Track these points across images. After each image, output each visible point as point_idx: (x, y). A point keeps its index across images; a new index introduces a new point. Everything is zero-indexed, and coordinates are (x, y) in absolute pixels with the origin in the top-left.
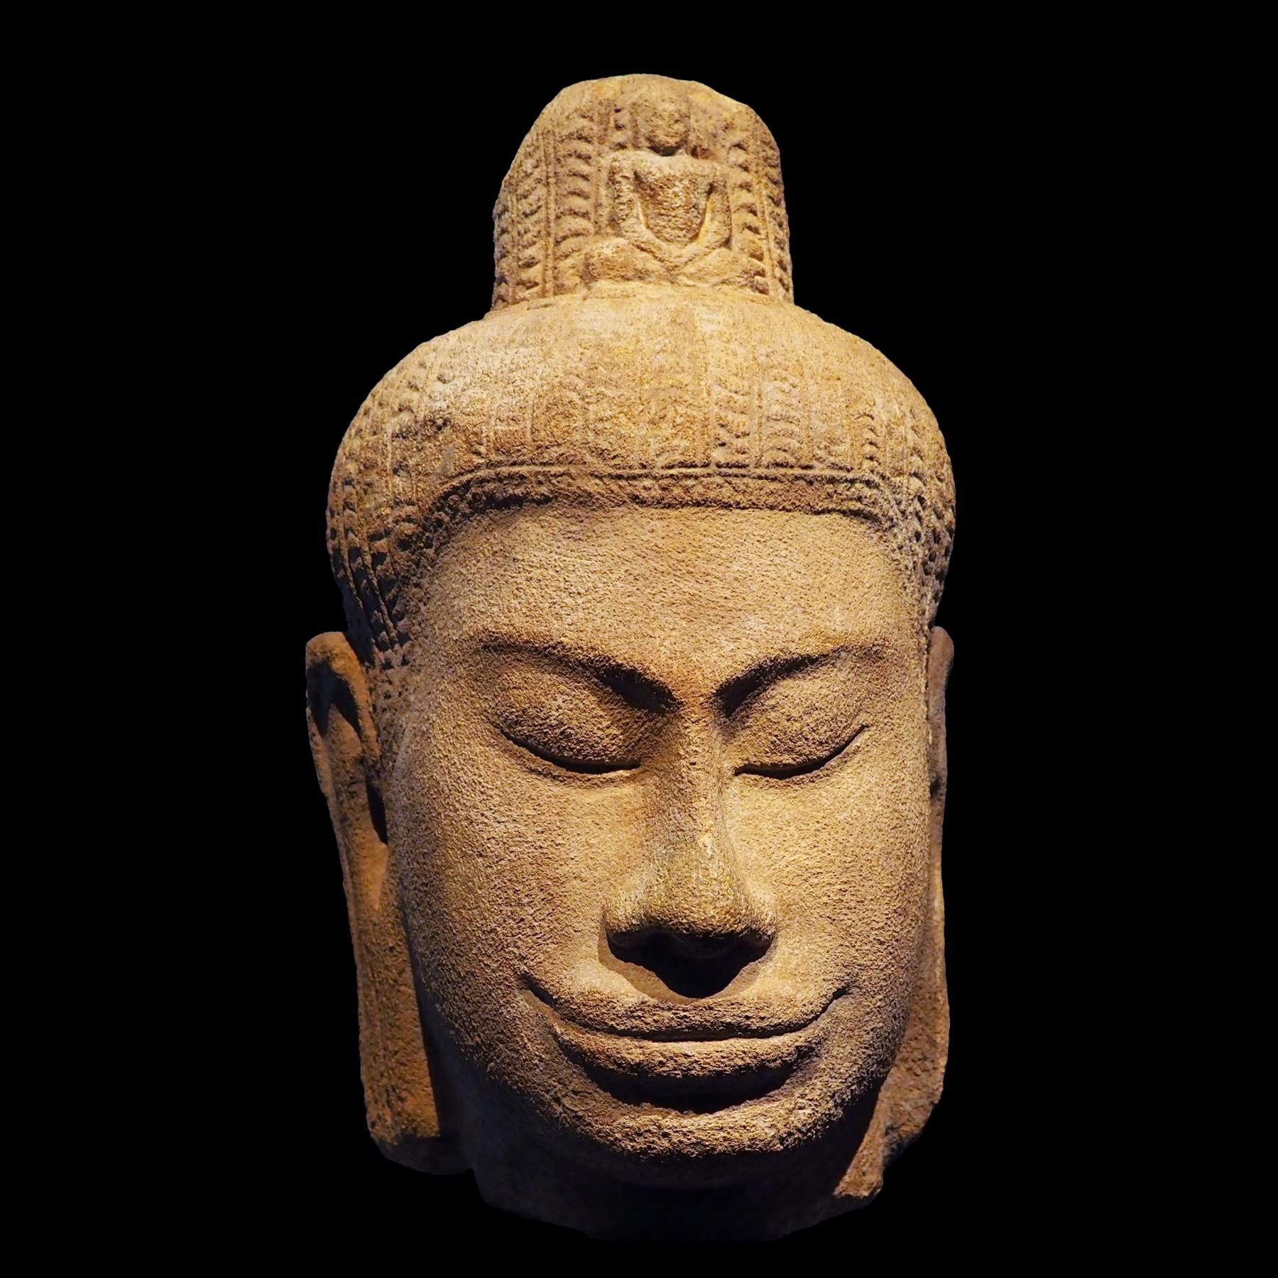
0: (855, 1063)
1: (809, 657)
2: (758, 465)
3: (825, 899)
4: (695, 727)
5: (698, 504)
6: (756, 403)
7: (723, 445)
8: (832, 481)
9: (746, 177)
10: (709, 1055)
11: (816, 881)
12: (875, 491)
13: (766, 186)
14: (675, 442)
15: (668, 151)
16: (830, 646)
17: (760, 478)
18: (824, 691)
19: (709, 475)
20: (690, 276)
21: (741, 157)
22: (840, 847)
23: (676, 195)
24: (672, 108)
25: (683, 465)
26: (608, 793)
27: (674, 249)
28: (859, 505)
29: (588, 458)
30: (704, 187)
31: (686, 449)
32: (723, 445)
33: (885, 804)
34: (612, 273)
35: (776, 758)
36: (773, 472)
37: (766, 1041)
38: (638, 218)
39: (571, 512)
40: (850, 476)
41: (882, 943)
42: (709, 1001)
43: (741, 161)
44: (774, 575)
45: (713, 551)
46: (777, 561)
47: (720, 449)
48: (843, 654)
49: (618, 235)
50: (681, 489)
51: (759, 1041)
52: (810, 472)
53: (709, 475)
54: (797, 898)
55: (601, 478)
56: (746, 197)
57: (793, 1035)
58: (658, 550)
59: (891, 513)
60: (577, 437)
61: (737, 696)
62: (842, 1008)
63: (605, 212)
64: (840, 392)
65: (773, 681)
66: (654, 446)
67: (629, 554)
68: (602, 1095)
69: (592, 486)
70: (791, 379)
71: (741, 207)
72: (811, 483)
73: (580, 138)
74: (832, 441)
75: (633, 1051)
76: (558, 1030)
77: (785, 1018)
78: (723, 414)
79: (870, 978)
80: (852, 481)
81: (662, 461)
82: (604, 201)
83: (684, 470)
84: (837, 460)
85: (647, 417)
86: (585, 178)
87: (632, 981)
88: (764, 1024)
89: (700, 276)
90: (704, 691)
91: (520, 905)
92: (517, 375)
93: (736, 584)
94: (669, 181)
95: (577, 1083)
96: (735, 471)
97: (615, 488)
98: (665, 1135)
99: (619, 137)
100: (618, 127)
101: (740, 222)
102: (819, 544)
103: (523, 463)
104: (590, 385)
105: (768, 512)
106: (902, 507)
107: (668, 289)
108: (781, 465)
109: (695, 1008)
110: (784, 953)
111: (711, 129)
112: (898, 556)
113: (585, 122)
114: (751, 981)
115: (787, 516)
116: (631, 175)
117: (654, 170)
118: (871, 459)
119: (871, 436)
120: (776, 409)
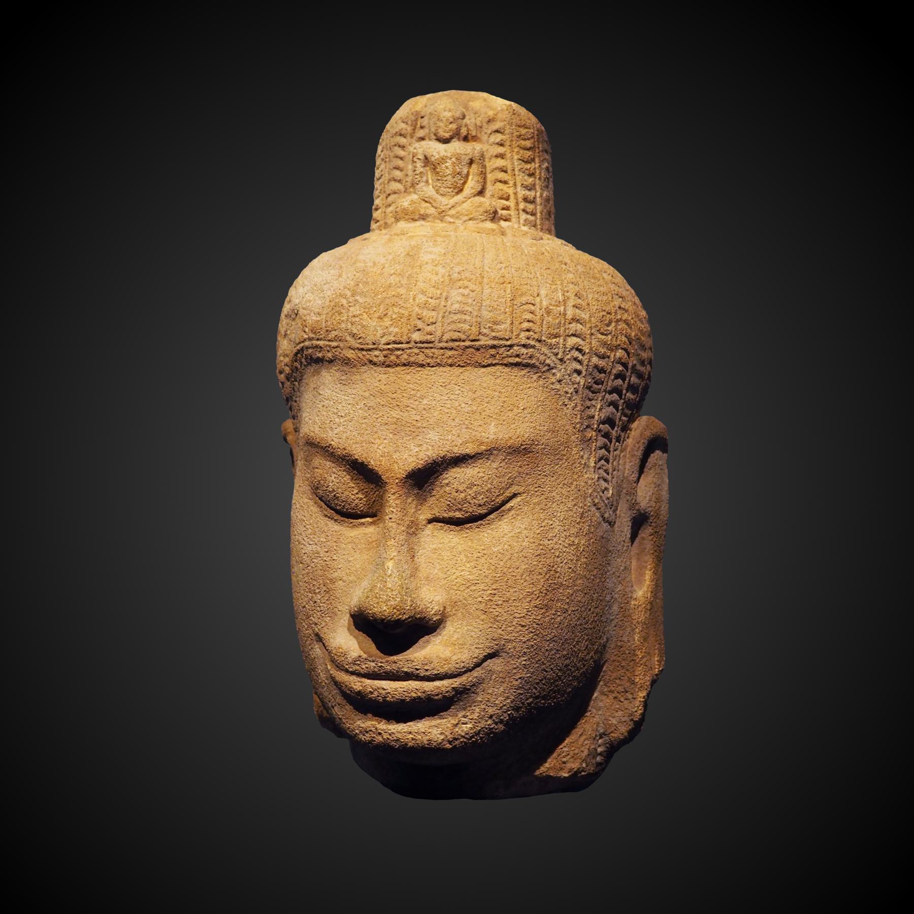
0: (508, 698)
1: (468, 455)
2: (440, 341)
3: (480, 599)
4: (393, 497)
5: (404, 365)
6: (443, 303)
7: (419, 330)
8: (494, 347)
9: (501, 150)
10: (396, 690)
11: (473, 588)
12: (531, 350)
13: (518, 153)
14: (391, 329)
15: (446, 141)
16: (484, 448)
17: (442, 348)
18: (481, 475)
19: (410, 348)
20: (452, 216)
21: (498, 138)
22: (493, 568)
23: (447, 168)
24: (448, 114)
25: (395, 342)
26: (361, 531)
27: (444, 200)
28: (517, 359)
29: (348, 338)
30: (466, 160)
31: (397, 333)
32: (419, 330)
33: (532, 540)
34: (407, 217)
35: (451, 514)
36: (451, 344)
37: (431, 683)
38: (427, 182)
39: (342, 368)
40: (509, 343)
41: (523, 626)
42: (395, 658)
43: (498, 140)
44: (449, 406)
45: (412, 392)
46: (452, 397)
47: (418, 332)
48: (495, 452)
49: (415, 193)
50: (395, 357)
51: (427, 683)
52: (477, 343)
53: (410, 348)
54: (461, 598)
55: (354, 349)
56: (500, 163)
57: (451, 681)
58: (382, 392)
59: (548, 361)
60: (343, 325)
61: (423, 479)
62: (494, 664)
63: (409, 179)
64: (508, 291)
65: (446, 469)
66: (380, 332)
67: (367, 394)
68: (349, 707)
69: (350, 354)
70: (472, 286)
71: (495, 169)
72: (478, 350)
73: (401, 135)
74: (495, 323)
75: (357, 684)
76: (329, 667)
77: (442, 670)
78: (420, 312)
79: (515, 648)
80: (511, 346)
81: (384, 340)
82: (410, 173)
83: (396, 346)
84: (497, 334)
85: (377, 315)
86: (401, 159)
87: (359, 643)
88: (428, 673)
89: (457, 216)
90: (398, 476)
91: (315, 593)
92: (326, 287)
93: (424, 412)
94: (443, 160)
95: (339, 698)
96: (426, 345)
97: (360, 355)
98: (380, 734)
99: (421, 133)
100: (422, 127)
101: (494, 178)
102: (485, 385)
103: (321, 339)
104: (353, 295)
105: (449, 368)
106: (559, 356)
107: (440, 225)
108: (456, 340)
109: (387, 662)
110: (450, 631)
111: (479, 124)
112: (558, 386)
113: (403, 126)
114: (423, 647)
115: (461, 370)
116: (421, 157)
117: (435, 154)
118: (528, 330)
119: (529, 316)
120: (456, 306)
